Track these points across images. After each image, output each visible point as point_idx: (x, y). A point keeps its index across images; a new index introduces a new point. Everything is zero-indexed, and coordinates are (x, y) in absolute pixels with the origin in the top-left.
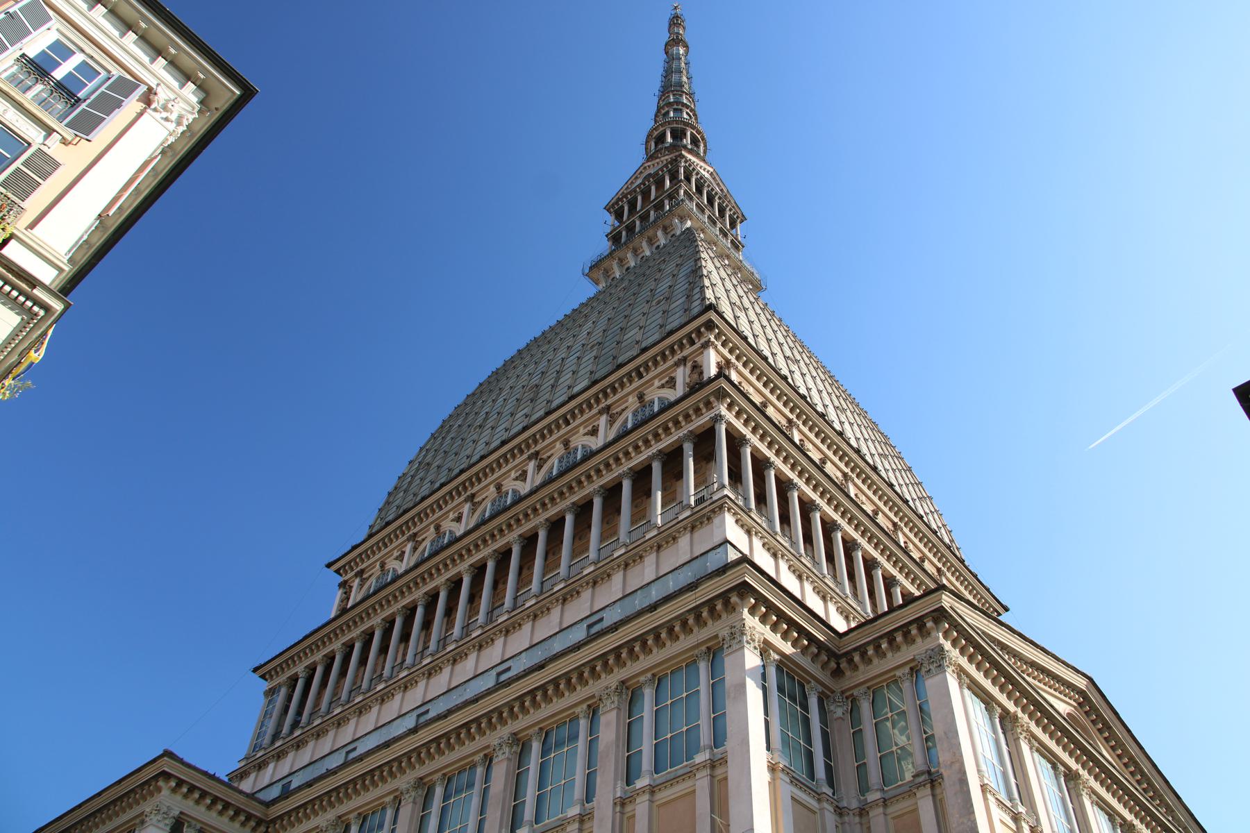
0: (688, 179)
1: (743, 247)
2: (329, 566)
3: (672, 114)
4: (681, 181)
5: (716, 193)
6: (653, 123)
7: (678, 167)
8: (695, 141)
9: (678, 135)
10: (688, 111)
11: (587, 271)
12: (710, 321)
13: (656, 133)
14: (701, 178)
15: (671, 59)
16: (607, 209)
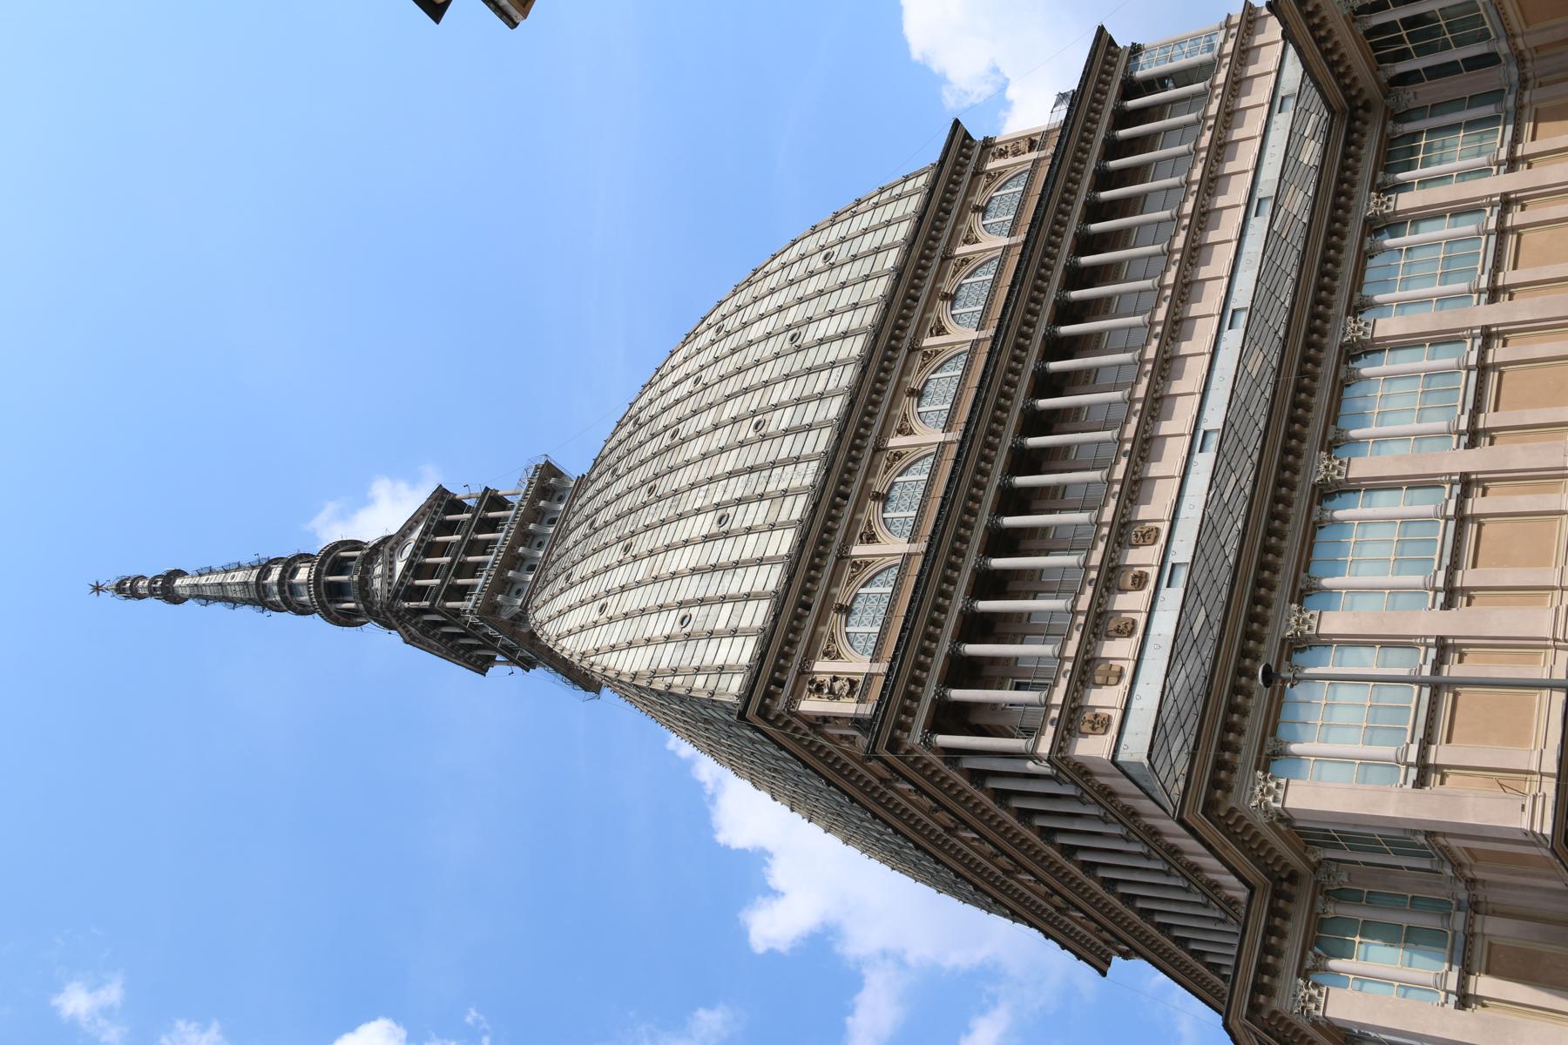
0: (421, 593)
1: (487, 489)
2: (1104, 974)
3: (305, 598)
4: (432, 605)
5: (421, 540)
6: (316, 615)
7: (408, 609)
8: (340, 566)
9: (337, 591)
10: (287, 575)
11: (593, 694)
12: (758, 714)
13: (342, 619)
14: (408, 567)
15: (201, 596)
16: (482, 671)
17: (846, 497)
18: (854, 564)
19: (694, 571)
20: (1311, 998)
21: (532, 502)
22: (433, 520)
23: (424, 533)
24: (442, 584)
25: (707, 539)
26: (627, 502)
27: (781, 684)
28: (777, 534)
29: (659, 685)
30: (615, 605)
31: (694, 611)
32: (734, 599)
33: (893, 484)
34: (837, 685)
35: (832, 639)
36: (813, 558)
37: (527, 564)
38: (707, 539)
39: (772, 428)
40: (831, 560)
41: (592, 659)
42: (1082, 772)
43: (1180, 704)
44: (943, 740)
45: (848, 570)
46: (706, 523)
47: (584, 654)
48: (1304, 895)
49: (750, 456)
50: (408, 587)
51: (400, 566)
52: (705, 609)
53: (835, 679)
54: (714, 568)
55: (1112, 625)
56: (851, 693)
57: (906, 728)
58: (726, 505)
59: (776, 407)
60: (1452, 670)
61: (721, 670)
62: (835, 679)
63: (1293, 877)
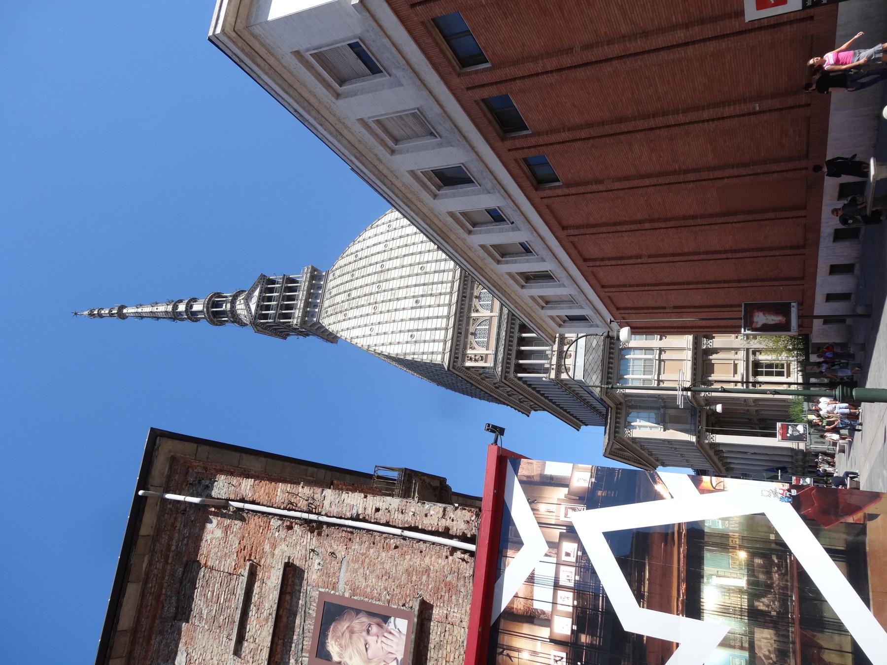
0: (266, 317)
1: (284, 275)
2: (528, 416)
4: (274, 321)
10: (189, 308)
12: (453, 368)
14: (258, 306)
17: (465, 297)
18: (473, 319)
19: (410, 319)
20: (629, 433)
21: (310, 282)
22: (262, 287)
23: (261, 292)
24: (276, 313)
25: (412, 308)
26: (367, 290)
27: (457, 358)
28: (441, 308)
29: (409, 358)
30: (376, 329)
31: (415, 333)
32: (431, 330)
33: (481, 293)
34: (477, 358)
35: (471, 343)
36: (459, 317)
37: (312, 305)
38: (412, 308)
39: (428, 270)
40: (465, 318)
41: (374, 348)
42: (562, 380)
43: (593, 365)
44: (520, 375)
45: (471, 321)
46: (411, 303)
47: (369, 346)
48: (624, 407)
49: (422, 279)
50: (259, 314)
51: (253, 307)
52: (419, 333)
53: (475, 356)
54: (419, 319)
55: (566, 341)
56: (482, 360)
57: (508, 372)
58: (418, 296)
59: (428, 262)
60: (663, 357)
61: (432, 353)
62: (475, 356)
63: (621, 404)
